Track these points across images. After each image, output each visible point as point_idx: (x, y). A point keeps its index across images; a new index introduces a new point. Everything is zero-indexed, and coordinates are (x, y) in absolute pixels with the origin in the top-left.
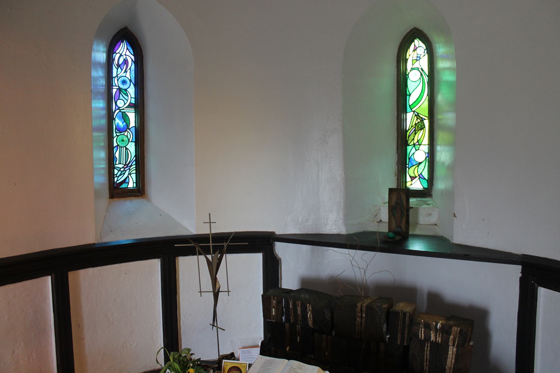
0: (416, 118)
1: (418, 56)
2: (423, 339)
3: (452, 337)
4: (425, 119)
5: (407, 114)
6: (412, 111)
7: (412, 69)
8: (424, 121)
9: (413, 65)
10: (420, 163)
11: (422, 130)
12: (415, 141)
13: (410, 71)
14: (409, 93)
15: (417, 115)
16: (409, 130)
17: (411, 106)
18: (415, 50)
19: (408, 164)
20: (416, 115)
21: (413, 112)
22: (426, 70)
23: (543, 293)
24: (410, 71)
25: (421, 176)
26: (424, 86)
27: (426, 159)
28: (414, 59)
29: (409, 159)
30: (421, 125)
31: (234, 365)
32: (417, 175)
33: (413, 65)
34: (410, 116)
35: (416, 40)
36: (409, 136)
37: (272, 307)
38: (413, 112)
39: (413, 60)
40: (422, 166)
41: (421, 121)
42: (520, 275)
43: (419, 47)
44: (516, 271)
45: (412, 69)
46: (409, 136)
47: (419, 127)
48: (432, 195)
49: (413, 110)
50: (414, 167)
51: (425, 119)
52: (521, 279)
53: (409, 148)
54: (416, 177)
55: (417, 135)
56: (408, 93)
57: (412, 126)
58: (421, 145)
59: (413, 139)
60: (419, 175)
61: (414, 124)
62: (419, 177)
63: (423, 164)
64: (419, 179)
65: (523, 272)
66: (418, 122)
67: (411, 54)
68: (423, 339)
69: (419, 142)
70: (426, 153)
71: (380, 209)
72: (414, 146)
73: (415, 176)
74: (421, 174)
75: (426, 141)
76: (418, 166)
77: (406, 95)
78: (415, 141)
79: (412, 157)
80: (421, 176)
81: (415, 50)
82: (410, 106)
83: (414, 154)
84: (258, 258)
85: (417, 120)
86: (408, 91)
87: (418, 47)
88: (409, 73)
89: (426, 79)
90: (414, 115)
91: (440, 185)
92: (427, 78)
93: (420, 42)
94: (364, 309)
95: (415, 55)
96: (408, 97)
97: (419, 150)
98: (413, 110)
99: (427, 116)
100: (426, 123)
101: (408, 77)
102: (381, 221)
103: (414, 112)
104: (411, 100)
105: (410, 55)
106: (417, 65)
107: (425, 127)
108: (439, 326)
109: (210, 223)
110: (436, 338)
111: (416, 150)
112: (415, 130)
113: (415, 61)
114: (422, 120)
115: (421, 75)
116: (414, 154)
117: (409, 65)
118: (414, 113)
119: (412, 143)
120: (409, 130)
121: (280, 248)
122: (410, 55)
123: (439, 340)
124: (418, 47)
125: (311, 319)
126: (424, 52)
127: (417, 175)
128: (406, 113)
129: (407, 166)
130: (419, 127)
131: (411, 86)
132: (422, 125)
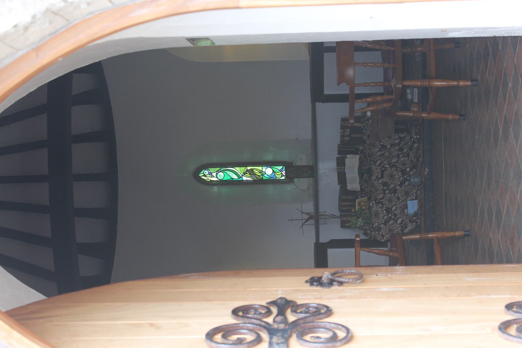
0: (246, 175)
1: (209, 174)
2: (349, 138)
3: (346, 125)
4: (247, 169)
5: (244, 180)
6: (242, 177)
7: (217, 177)
8: (248, 169)
9: (214, 177)
10: (273, 171)
11: (254, 170)
12: (260, 174)
13: (218, 178)
14: (231, 179)
15: (245, 173)
16: (253, 179)
17: (239, 177)
18: (205, 176)
19: (274, 178)
20: (244, 175)
21: (243, 177)
22: (218, 169)
23: (326, 92)
24: (218, 178)
25: (281, 171)
26: (226, 170)
27: (270, 168)
28: (210, 177)
29: (271, 178)
30: (251, 171)
31: (358, 205)
32: (281, 173)
33: (214, 177)
34: (245, 178)
35: (200, 175)
36: (257, 178)
37: (347, 220)
38: (243, 177)
39: (211, 177)
40: (275, 170)
41: (248, 172)
42: (321, 103)
43: (204, 174)
44: (319, 105)
45: (217, 177)
46: (257, 178)
47: (251, 172)
48: (292, 162)
49: (241, 176)
50: (276, 175)
51: (247, 169)
52: (322, 103)
53: (264, 178)
54: (282, 173)
55: (256, 173)
56: (231, 180)
57: (251, 177)
58: (262, 171)
59: (259, 175)
60: (281, 172)
61: (250, 176)
62: (282, 172)
63: (274, 169)
64: (283, 171)
65: (319, 102)
66: (249, 173)
67: (209, 178)
68: (349, 138)
69: (260, 172)
70: (267, 168)
71: (301, 189)
72: (263, 175)
73: (281, 174)
74: (279, 170)
75: (260, 168)
76: (275, 172)
77: (232, 180)
78: (260, 174)
79: (269, 176)
80: (281, 170)
81: (205, 176)
82: (239, 178)
83: (268, 175)
84: (331, 252)
85: (247, 174)
86: (230, 180)
87: (203, 174)
88: (219, 179)
89: (223, 169)
90: (244, 176)
91: (286, 158)
92: (223, 168)
93: (201, 173)
94: (339, 167)
95: (208, 176)
96: (233, 180)
97: (265, 172)
98: (241, 176)
99: (245, 167)
100: (249, 168)
101: (221, 179)
102: (307, 188)
103: (242, 176)
104: (235, 177)
105: (208, 179)
106: (214, 174)
107: (252, 169)
108: (342, 131)
109: (292, 220)
110: (348, 132)
111: (266, 174)
112: (253, 175)
113: (212, 176)
114: (247, 170)
115: (220, 172)
116: (268, 175)
117: (215, 179)
118: (243, 176)
119: (261, 176)
120: (253, 179)
121: (324, 239)
122: (208, 179)
123: (348, 130)
124: (203, 174)
125: (350, 196)
126: (207, 170)
127: (281, 173)
128: (243, 180)
129: (275, 179)
130: (251, 172)
131: (227, 178)
132: (250, 170)
